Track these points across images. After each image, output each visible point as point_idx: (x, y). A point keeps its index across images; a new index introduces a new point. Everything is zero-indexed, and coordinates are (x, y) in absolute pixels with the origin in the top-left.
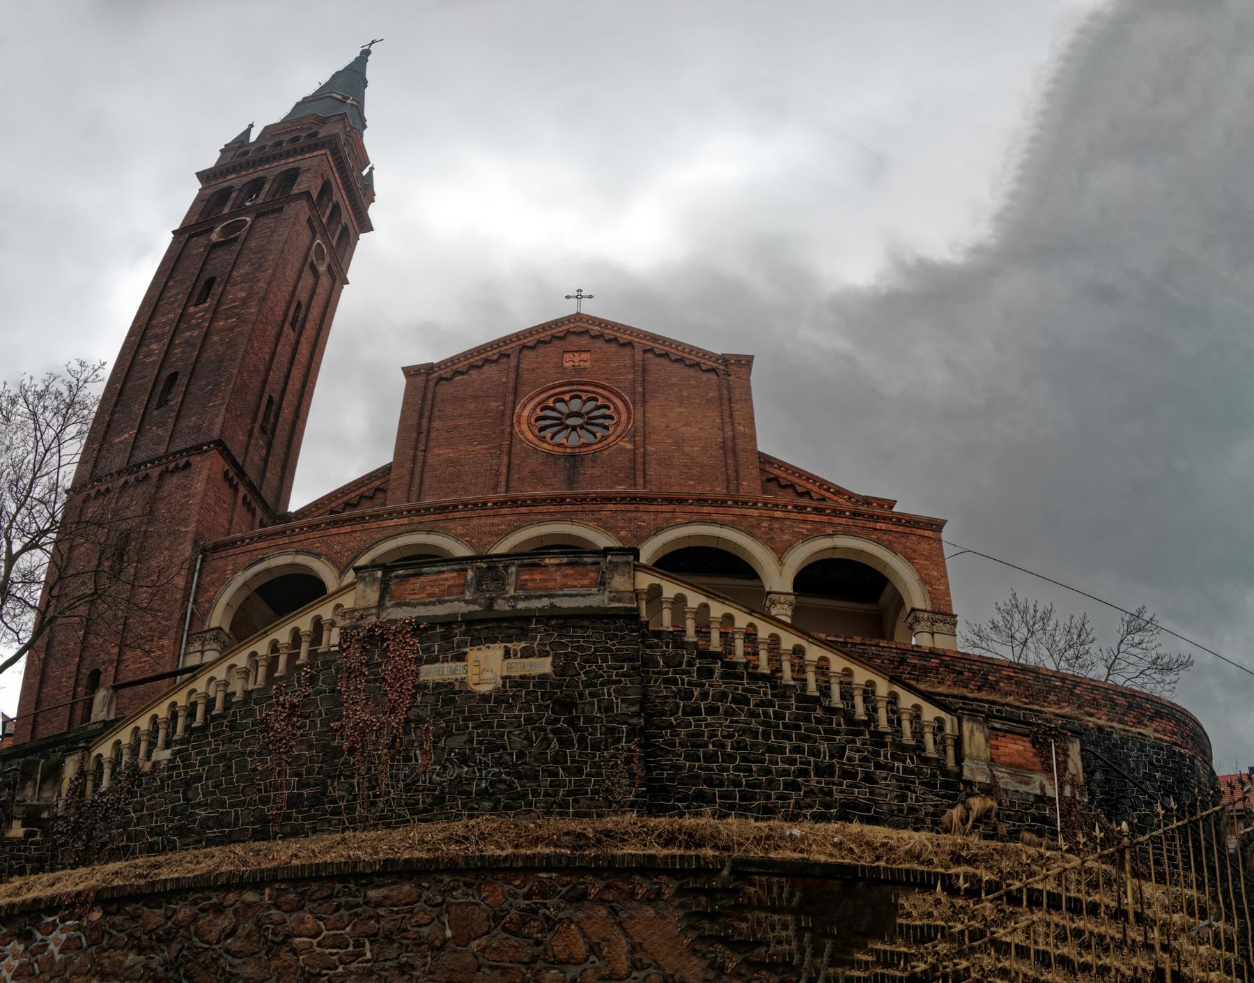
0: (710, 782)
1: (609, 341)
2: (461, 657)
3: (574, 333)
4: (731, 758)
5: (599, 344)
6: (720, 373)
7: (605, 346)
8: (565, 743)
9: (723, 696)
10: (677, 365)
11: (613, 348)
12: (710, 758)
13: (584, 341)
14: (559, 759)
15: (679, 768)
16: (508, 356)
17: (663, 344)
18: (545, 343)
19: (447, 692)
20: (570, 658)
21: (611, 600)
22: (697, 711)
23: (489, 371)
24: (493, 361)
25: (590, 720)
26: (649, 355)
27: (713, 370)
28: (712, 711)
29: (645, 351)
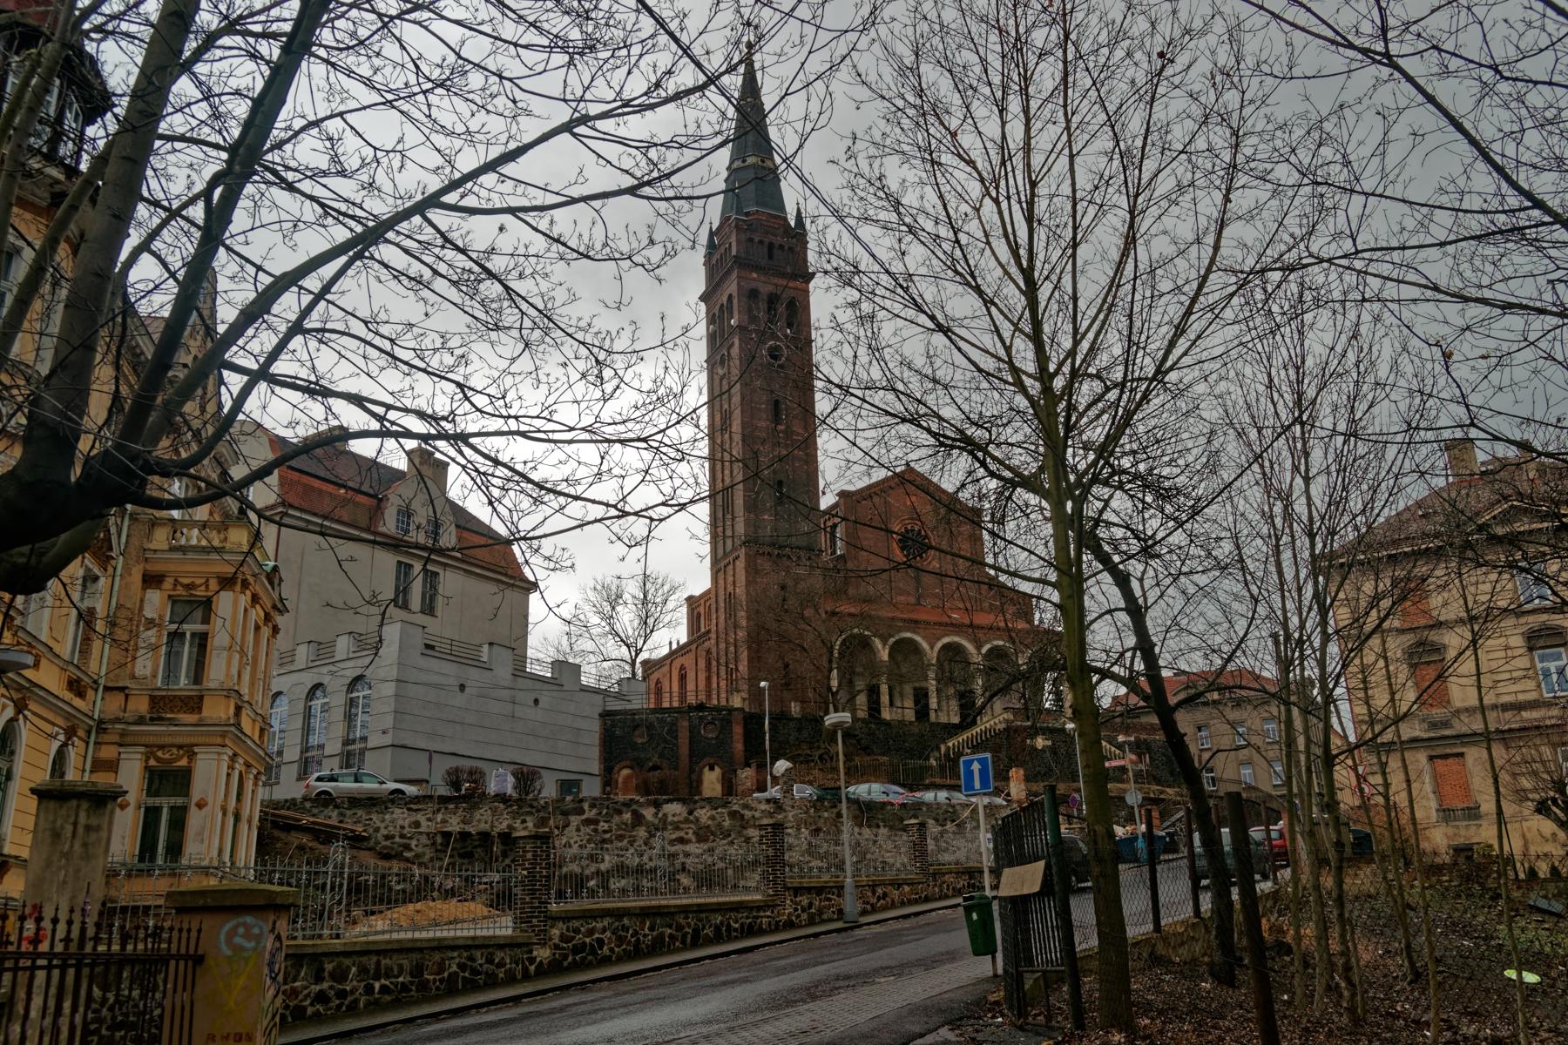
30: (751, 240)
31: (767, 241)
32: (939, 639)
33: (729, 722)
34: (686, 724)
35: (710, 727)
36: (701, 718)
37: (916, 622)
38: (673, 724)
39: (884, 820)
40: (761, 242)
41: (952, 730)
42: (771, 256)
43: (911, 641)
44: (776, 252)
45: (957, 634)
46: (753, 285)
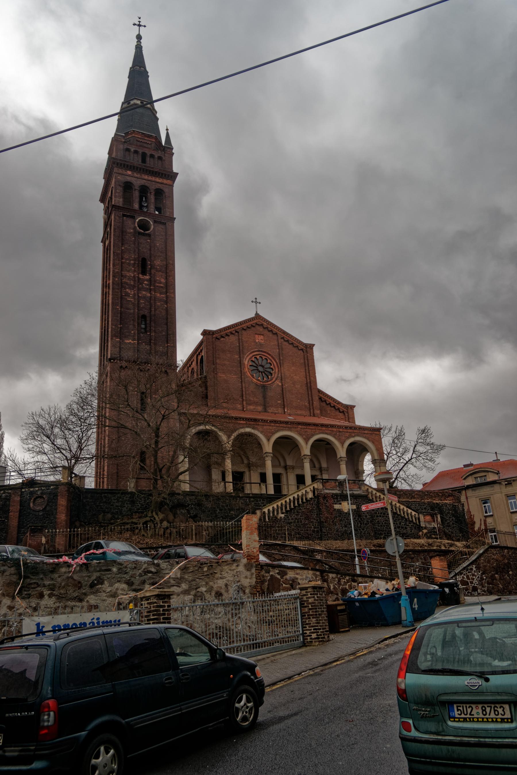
0: (381, 530)
1: (269, 331)
2: (340, 504)
3: (258, 325)
4: (384, 526)
5: (266, 332)
6: (304, 351)
7: (268, 333)
8: (361, 524)
9: (381, 513)
10: (291, 346)
11: (270, 334)
12: (381, 526)
13: (261, 329)
14: (360, 527)
15: (376, 528)
16: (238, 332)
17: (286, 335)
18: (249, 328)
19: (340, 511)
20: (358, 505)
21: (363, 492)
22: (378, 517)
23: (233, 339)
24: (233, 334)
25: (364, 519)
26: (282, 340)
27: (302, 350)
28: (380, 516)
29: (282, 338)
30: (128, 150)
31: (140, 151)
32: (273, 433)
33: (56, 495)
34: (18, 499)
35: (39, 501)
36: (32, 493)
37: (255, 420)
38: (8, 499)
39: (52, 588)
40: (136, 152)
41: (270, 499)
42: (144, 161)
43: (250, 435)
44: (148, 159)
45: (290, 429)
46: (129, 179)
